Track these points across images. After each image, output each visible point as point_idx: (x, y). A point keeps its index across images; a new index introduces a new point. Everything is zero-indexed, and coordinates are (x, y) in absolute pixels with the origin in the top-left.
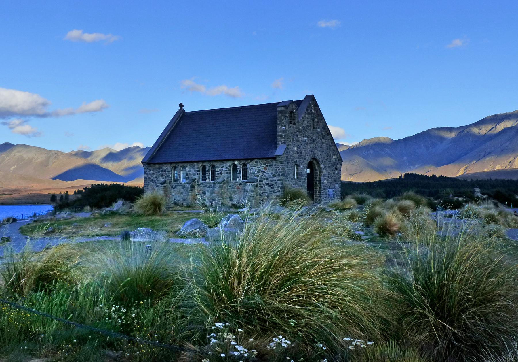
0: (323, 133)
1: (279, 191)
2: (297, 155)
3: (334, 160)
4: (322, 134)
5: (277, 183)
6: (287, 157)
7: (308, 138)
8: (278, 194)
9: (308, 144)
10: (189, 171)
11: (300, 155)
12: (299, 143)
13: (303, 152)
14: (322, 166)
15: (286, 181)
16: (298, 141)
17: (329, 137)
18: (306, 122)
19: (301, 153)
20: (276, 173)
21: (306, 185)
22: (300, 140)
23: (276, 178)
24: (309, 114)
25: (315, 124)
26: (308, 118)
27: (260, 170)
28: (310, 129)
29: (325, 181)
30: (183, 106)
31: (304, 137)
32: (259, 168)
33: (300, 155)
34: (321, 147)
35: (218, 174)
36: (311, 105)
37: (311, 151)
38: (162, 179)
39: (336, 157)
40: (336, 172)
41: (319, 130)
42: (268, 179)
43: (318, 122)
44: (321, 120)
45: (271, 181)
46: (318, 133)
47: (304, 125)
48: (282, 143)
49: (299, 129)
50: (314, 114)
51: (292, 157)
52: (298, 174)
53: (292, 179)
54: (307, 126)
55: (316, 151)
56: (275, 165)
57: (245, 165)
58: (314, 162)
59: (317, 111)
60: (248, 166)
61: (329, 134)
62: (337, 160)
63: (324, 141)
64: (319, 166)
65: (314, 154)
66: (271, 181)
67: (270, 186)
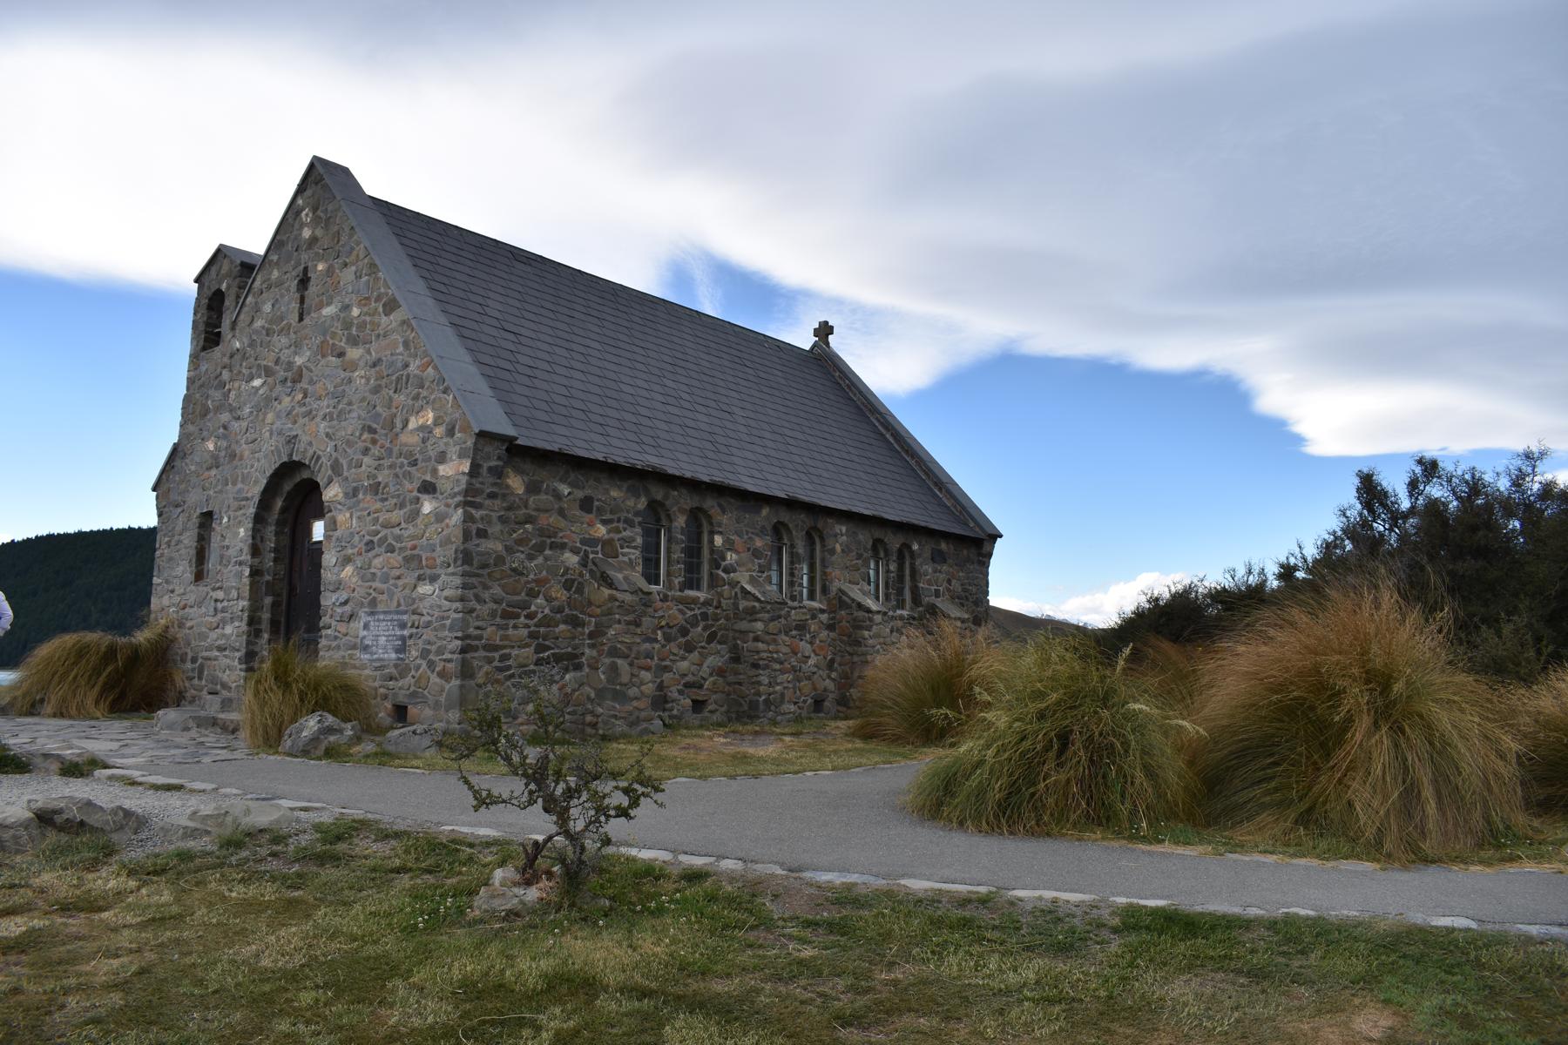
7: (269, 372)
40: (427, 507)
43: (330, 272)
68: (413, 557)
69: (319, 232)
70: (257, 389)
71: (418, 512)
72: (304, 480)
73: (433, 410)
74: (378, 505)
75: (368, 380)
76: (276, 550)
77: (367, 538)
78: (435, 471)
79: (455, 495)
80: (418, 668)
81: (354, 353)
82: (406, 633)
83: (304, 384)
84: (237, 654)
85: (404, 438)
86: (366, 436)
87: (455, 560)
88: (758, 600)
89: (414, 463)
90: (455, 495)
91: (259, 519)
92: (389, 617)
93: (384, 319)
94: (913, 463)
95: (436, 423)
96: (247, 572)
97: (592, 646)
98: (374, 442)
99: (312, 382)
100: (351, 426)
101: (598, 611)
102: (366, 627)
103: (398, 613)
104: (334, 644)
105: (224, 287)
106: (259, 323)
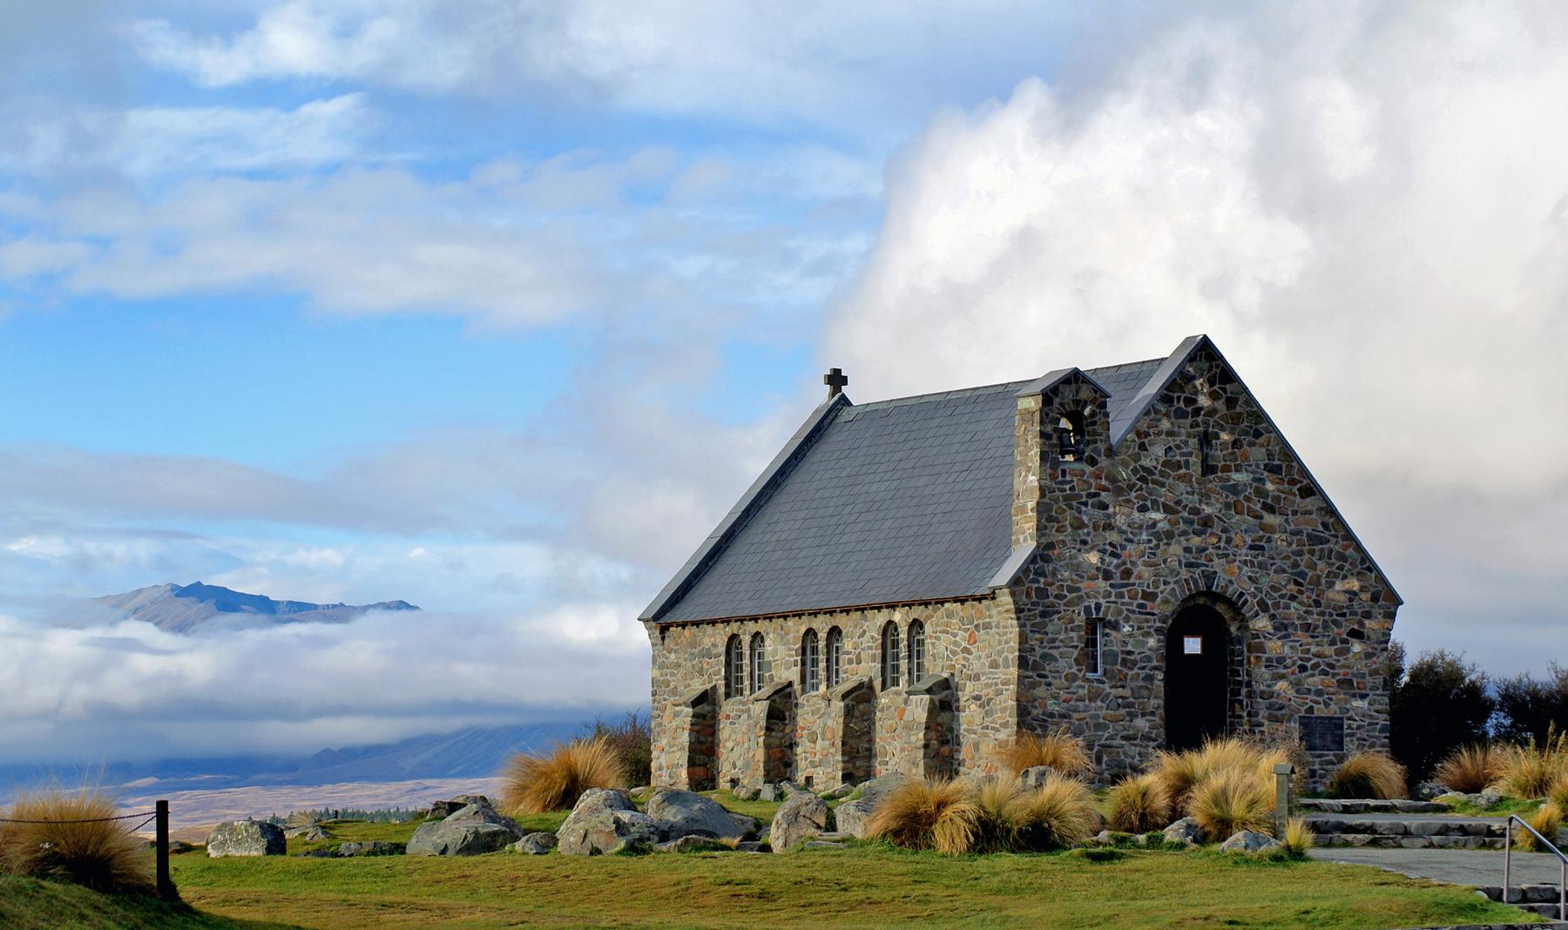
0: (1270, 486)
1: (1005, 725)
2: (1102, 585)
3: (1343, 598)
4: (1261, 493)
5: (999, 693)
6: (1042, 593)
7: (1167, 509)
8: (1002, 736)
9: (1169, 535)
10: (775, 652)
11: (1117, 580)
12: (1114, 537)
13: (1140, 568)
14: (1262, 623)
15: (1034, 686)
16: (1109, 527)
17: (1310, 503)
18: (1158, 451)
19: (1127, 574)
20: (1000, 653)
21: (1156, 702)
22: (1120, 521)
23: (1001, 674)
24: (1181, 414)
25: (1218, 455)
26: (1170, 433)
27: (956, 644)
28: (1186, 478)
29: (1281, 685)
30: (844, 381)
31: (1143, 509)
32: (955, 635)
33: (1117, 580)
34: (1251, 548)
35: (850, 662)
37: (1189, 565)
38: (698, 686)
39: (1355, 584)
41: (1240, 477)
42: (977, 677)
43: (1235, 444)
44: (1258, 434)
45: (987, 686)
46: (1234, 489)
47: (1146, 462)
48: (1025, 540)
49: (1113, 480)
50: (1212, 412)
51: (1071, 590)
52: (1104, 654)
53: (1071, 678)
55: (1218, 564)
56: (997, 626)
57: (916, 625)
58: (1220, 608)
59: (1231, 402)
60: (928, 628)
61: (1310, 489)
62: (1365, 596)
63: (1269, 519)
64: (1244, 627)
65: (1210, 577)
66: (987, 686)
67: (982, 706)
70: (1154, 525)
71: (1348, 650)
75: (1290, 544)
78: (1361, 624)
84: (1152, 744)
85: (1330, 594)
86: (1292, 586)
89: (1343, 615)
93: (1298, 499)
95: (1362, 589)
96: (1160, 676)
98: (1301, 592)
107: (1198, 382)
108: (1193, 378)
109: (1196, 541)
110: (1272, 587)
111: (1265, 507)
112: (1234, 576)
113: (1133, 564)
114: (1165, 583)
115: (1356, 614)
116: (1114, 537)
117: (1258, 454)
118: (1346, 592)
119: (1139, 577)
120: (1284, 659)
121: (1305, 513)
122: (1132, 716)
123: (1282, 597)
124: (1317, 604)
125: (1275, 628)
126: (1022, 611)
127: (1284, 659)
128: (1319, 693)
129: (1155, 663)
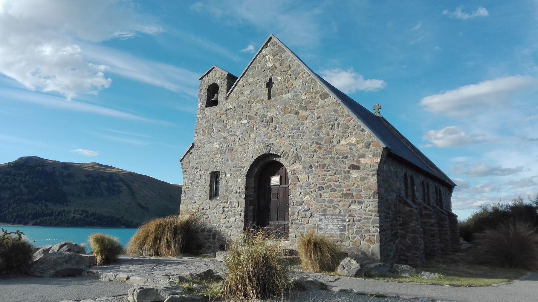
0: (303, 97)
3: (346, 148)
7: (250, 118)
12: (225, 134)
24: (259, 74)
29: (308, 197)
36: (264, 56)
39: (354, 140)
43: (285, 80)
54: (250, 98)
68: (348, 194)
69: (277, 64)
70: (244, 124)
71: (349, 177)
72: (276, 161)
73: (355, 137)
74: (325, 173)
75: (314, 124)
76: (254, 188)
77: (319, 185)
78: (358, 161)
79: (372, 171)
80: (354, 238)
81: (303, 113)
82: (345, 223)
83: (274, 123)
85: (337, 147)
87: (374, 196)
88: (431, 211)
89: (347, 157)
90: (372, 171)
91: (248, 176)
92: (334, 217)
94: (420, 157)
95: (358, 142)
97: (402, 229)
99: (278, 123)
100: (305, 141)
101: (404, 216)
102: (320, 220)
103: (340, 215)
104: (300, 227)
105: (218, 83)
106: (242, 98)
107: (267, 57)
108: (266, 55)
109: (264, 130)
110: (304, 147)
111: (301, 107)
112: (281, 146)
113: (235, 145)
114: (248, 152)
115: (355, 156)
116: (225, 134)
117: (298, 83)
118: (349, 144)
119: (236, 151)
120: (309, 184)
121: (322, 107)
122: (230, 216)
123: (308, 151)
124: (330, 153)
125: (305, 168)
126: (185, 171)
127: (309, 184)
128: (331, 201)
129: (240, 191)
